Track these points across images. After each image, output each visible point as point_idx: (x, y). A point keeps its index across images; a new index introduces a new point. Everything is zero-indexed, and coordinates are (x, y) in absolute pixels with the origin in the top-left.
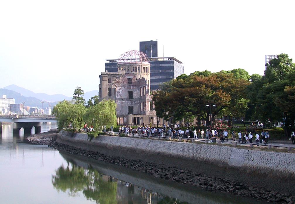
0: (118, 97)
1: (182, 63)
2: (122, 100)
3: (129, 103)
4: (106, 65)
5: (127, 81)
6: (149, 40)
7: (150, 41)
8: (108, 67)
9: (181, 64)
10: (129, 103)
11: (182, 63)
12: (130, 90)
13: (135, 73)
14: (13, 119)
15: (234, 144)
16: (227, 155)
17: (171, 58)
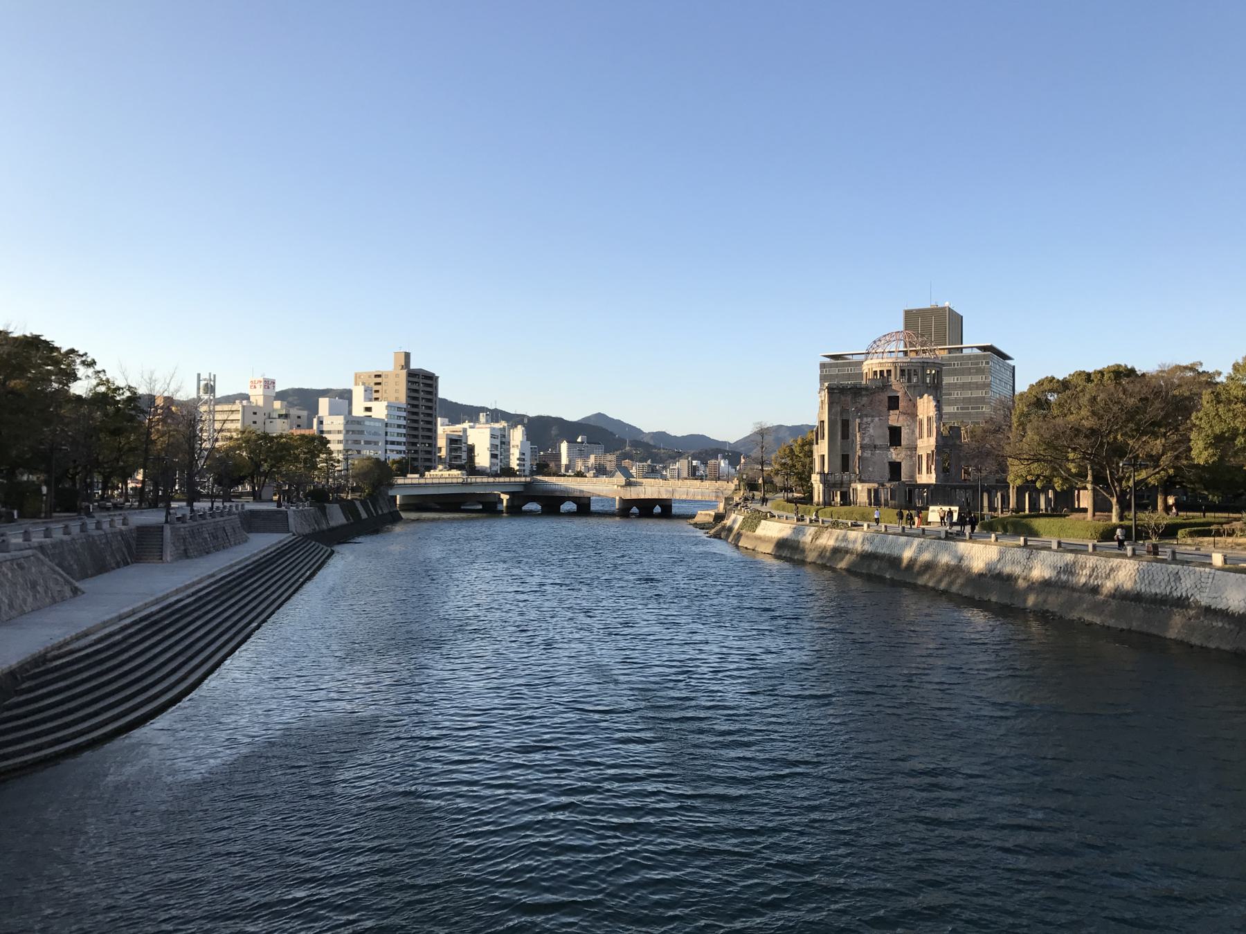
0: (865, 442)
2: (875, 447)
4: (823, 366)
5: (887, 404)
7: (928, 306)
8: (827, 371)
12: (895, 424)
16: (1199, 587)
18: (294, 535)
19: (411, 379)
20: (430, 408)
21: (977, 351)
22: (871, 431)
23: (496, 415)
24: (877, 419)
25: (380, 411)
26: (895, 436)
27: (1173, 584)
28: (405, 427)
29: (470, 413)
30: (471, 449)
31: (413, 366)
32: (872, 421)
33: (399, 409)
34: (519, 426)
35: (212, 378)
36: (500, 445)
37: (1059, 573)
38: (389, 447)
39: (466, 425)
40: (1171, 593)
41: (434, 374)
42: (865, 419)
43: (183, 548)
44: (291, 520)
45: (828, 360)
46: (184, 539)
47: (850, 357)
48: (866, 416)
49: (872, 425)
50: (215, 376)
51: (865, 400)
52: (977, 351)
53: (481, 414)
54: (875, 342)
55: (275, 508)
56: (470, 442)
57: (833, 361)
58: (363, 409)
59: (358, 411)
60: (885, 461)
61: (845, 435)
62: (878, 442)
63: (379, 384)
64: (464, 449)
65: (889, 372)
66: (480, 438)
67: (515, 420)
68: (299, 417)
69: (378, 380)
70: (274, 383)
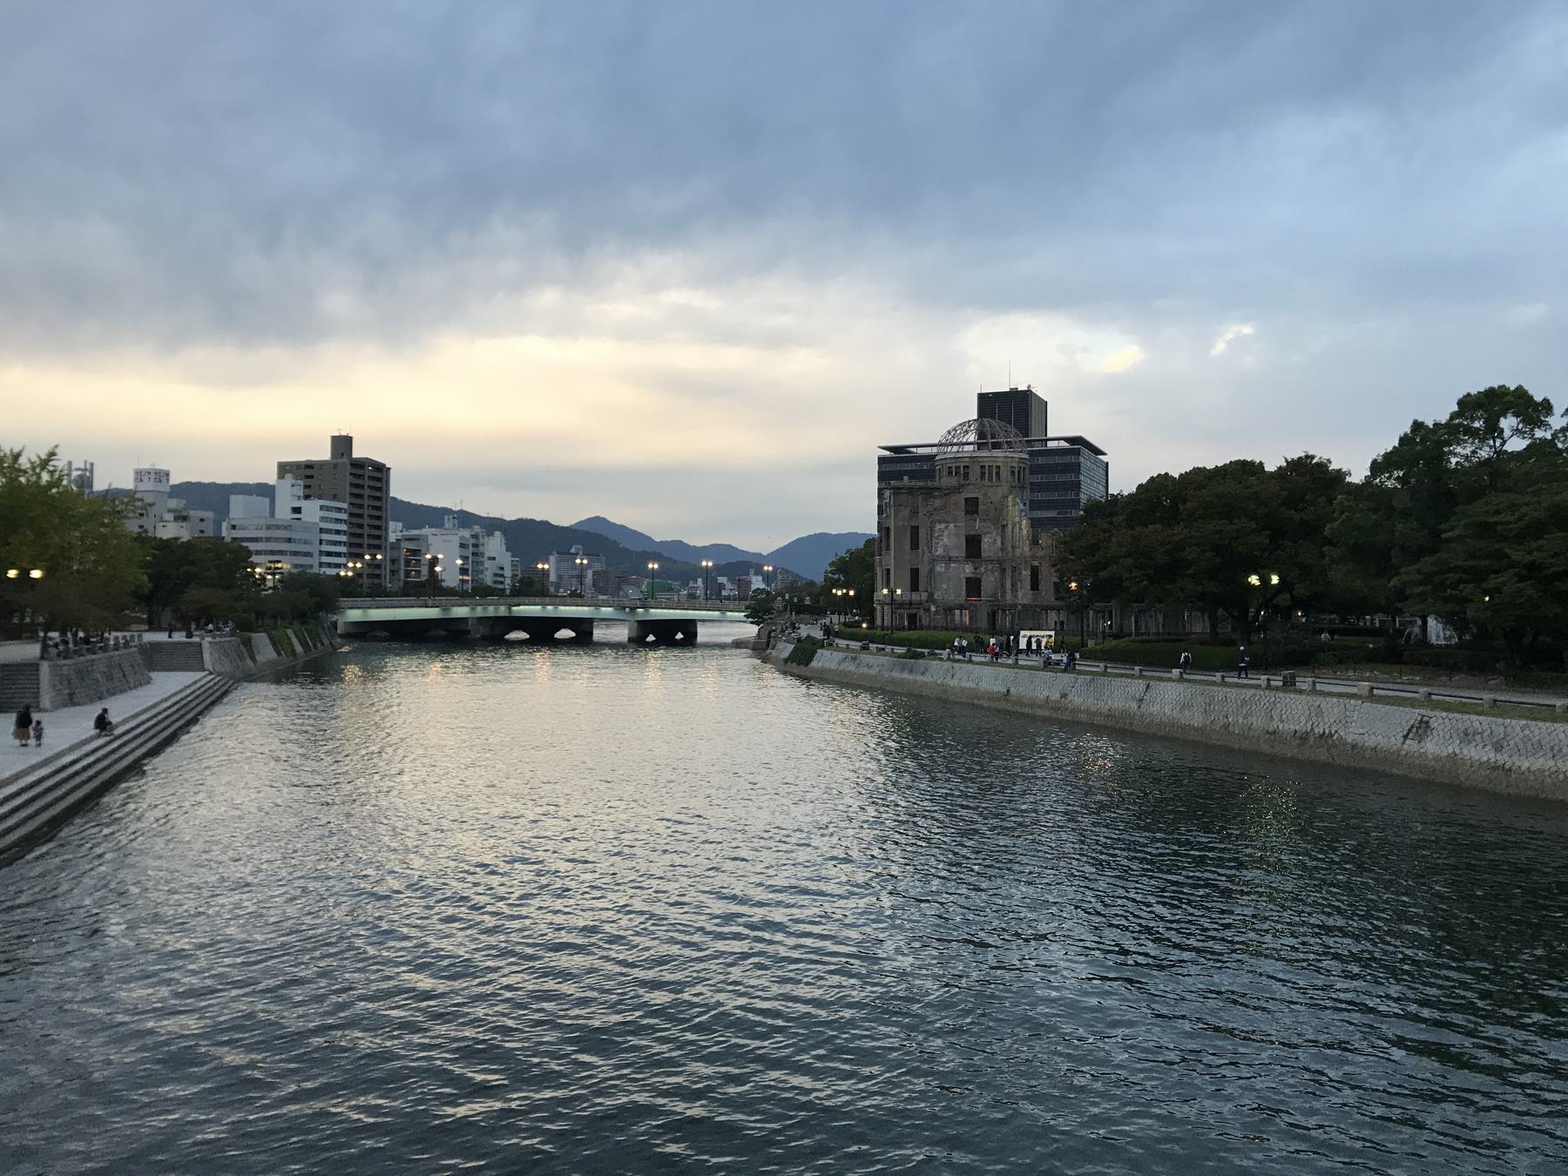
0: (938, 553)
1: (1104, 454)
3: (968, 569)
4: (882, 460)
6: (1004, 388)
8: (888, 468)
10: (968, 569)
11: (1104, 454)
12: (972, 533)
14: (627, 610)
15: (1366, 693)
18: (211, 673)
19: (354, 471)
20: (379, 508)
21: (1063, 444)
23: (465, 519)
24: (952, 526)
26: (973, 546)
27: (1314, 719)
28: (345, 533)
29: (434, 517)
31: (357, 453)
32: (946, 528)
34: (497, 534)
35: (88, 467)
38: (325, 559)
39: (426, 531)
40: (1312, 729)
41: (384, 465)
42: (938, 526)
43: (67, 691)
44: (207, 656)
45: (887, 453)
46: (69, 681)
47: (914, 450)
48: (940, 522)
49: (946, 533)
50: (92, 464)
51: (938, 503)
53: (446, 517)
54: (949, 432)
55: (184, 639)
58: (289, 510)
60: (962, 576)
61: (915, 545)
62: (953, 554)
63: (311, 477)
65: (966, 467)
67: (493, 525)
68: (202, 520)
69: (309, 472)
70: (168, 475)
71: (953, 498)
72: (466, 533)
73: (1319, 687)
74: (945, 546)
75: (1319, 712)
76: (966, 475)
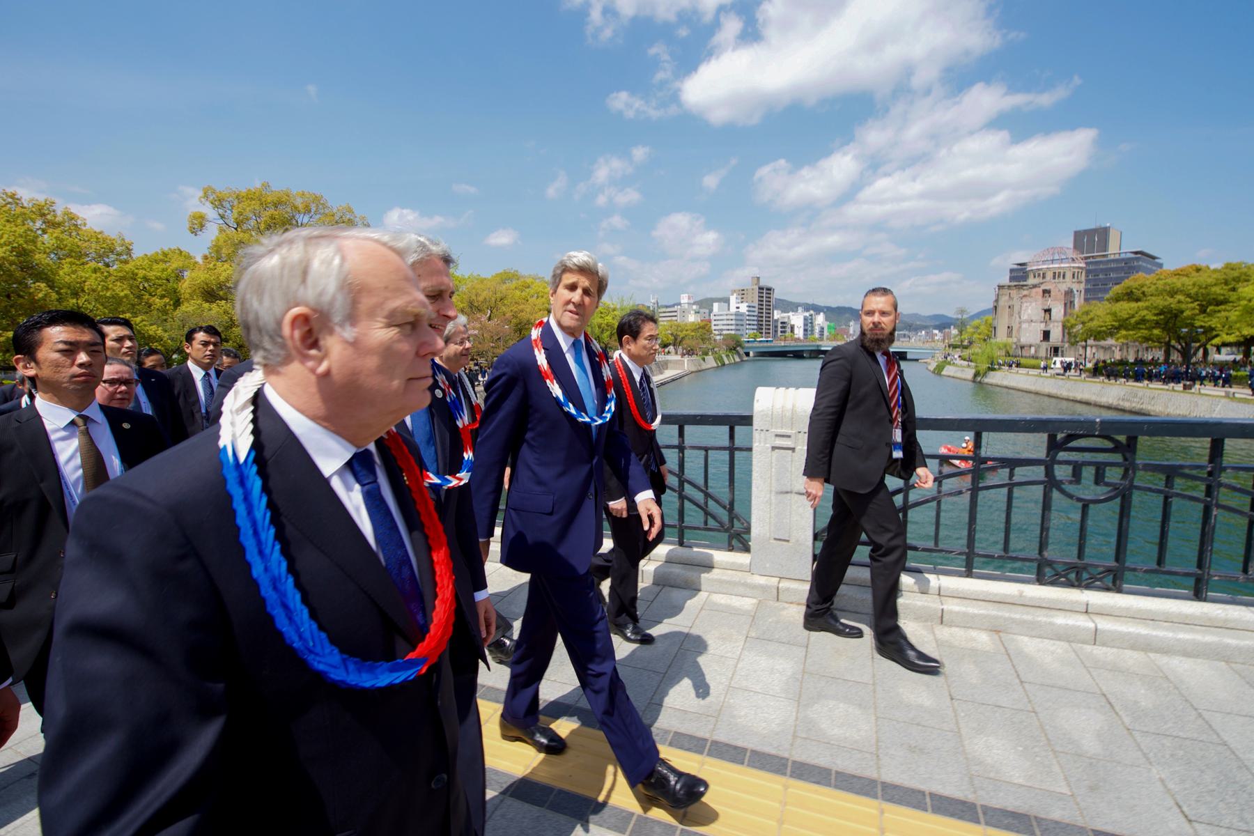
3: (1043, 327)
4: (1012, 271)
9: (1157, 260)
13: (1057, 280)
17: (1136, 253)
21: (1133, 256)
22: (1029, 311)
23: (807, 308)
25: (744, 308)
29: (790, 307)
30: (792, 328)
33: (754, 307)
34: (822, 314)
36: (808, 324)
37: (1119, 399)
39: (791, 314)
51: (1025, 292)
52: (1133, 256)
56: (792, 323)
57: (1019, 267)
59: (733, 310)
62: (1034, 319)
64: (789, 326)
66: (797, 320)
67: (818, 309)
71: (1034, 290)
72: (807, 314)
73: (1202, 391)
74: (1028, 315)
75: (1197, 405)
76: (1044, 277)
